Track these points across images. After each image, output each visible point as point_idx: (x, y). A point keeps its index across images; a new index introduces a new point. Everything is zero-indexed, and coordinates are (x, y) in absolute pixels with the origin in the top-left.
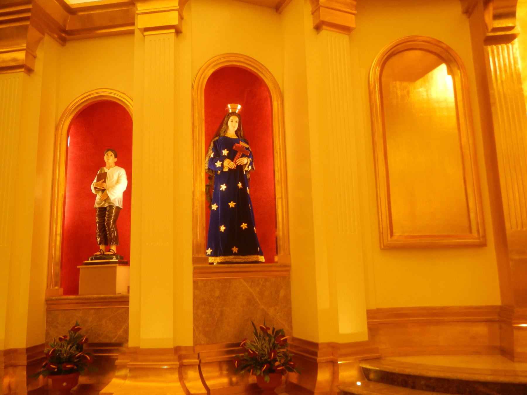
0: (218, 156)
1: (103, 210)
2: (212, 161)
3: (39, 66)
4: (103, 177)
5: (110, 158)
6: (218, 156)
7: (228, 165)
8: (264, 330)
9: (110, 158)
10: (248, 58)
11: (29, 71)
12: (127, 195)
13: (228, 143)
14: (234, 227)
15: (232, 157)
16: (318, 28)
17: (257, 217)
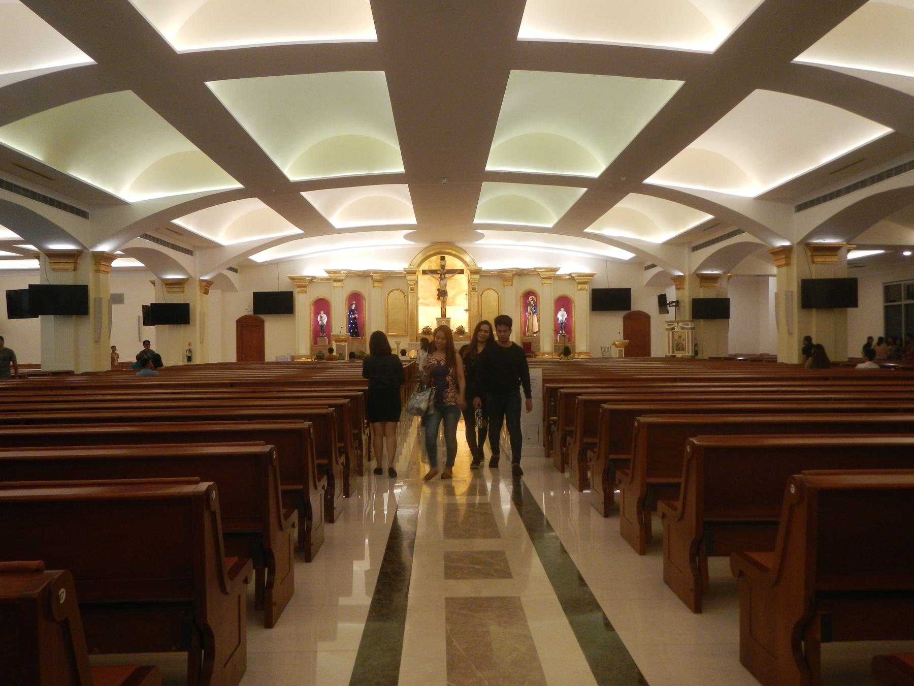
0: (350, 314)
1: (322, 326)
2: (349, 315)
3: (308, 292)
4: (321, 317)
5: (322, 312)
6: (350, 314)
7: (353, 316)
8: (361, 352)
9: (322, 312)
10: (358, 291)
11: (306, 292)
12: (329, 321)
13: (352, 311)
14: (354, 330)
15: (354, 314)
16: (374, 287)
17: (359, 328)
